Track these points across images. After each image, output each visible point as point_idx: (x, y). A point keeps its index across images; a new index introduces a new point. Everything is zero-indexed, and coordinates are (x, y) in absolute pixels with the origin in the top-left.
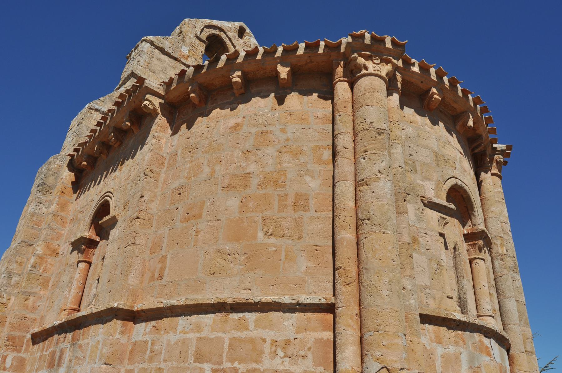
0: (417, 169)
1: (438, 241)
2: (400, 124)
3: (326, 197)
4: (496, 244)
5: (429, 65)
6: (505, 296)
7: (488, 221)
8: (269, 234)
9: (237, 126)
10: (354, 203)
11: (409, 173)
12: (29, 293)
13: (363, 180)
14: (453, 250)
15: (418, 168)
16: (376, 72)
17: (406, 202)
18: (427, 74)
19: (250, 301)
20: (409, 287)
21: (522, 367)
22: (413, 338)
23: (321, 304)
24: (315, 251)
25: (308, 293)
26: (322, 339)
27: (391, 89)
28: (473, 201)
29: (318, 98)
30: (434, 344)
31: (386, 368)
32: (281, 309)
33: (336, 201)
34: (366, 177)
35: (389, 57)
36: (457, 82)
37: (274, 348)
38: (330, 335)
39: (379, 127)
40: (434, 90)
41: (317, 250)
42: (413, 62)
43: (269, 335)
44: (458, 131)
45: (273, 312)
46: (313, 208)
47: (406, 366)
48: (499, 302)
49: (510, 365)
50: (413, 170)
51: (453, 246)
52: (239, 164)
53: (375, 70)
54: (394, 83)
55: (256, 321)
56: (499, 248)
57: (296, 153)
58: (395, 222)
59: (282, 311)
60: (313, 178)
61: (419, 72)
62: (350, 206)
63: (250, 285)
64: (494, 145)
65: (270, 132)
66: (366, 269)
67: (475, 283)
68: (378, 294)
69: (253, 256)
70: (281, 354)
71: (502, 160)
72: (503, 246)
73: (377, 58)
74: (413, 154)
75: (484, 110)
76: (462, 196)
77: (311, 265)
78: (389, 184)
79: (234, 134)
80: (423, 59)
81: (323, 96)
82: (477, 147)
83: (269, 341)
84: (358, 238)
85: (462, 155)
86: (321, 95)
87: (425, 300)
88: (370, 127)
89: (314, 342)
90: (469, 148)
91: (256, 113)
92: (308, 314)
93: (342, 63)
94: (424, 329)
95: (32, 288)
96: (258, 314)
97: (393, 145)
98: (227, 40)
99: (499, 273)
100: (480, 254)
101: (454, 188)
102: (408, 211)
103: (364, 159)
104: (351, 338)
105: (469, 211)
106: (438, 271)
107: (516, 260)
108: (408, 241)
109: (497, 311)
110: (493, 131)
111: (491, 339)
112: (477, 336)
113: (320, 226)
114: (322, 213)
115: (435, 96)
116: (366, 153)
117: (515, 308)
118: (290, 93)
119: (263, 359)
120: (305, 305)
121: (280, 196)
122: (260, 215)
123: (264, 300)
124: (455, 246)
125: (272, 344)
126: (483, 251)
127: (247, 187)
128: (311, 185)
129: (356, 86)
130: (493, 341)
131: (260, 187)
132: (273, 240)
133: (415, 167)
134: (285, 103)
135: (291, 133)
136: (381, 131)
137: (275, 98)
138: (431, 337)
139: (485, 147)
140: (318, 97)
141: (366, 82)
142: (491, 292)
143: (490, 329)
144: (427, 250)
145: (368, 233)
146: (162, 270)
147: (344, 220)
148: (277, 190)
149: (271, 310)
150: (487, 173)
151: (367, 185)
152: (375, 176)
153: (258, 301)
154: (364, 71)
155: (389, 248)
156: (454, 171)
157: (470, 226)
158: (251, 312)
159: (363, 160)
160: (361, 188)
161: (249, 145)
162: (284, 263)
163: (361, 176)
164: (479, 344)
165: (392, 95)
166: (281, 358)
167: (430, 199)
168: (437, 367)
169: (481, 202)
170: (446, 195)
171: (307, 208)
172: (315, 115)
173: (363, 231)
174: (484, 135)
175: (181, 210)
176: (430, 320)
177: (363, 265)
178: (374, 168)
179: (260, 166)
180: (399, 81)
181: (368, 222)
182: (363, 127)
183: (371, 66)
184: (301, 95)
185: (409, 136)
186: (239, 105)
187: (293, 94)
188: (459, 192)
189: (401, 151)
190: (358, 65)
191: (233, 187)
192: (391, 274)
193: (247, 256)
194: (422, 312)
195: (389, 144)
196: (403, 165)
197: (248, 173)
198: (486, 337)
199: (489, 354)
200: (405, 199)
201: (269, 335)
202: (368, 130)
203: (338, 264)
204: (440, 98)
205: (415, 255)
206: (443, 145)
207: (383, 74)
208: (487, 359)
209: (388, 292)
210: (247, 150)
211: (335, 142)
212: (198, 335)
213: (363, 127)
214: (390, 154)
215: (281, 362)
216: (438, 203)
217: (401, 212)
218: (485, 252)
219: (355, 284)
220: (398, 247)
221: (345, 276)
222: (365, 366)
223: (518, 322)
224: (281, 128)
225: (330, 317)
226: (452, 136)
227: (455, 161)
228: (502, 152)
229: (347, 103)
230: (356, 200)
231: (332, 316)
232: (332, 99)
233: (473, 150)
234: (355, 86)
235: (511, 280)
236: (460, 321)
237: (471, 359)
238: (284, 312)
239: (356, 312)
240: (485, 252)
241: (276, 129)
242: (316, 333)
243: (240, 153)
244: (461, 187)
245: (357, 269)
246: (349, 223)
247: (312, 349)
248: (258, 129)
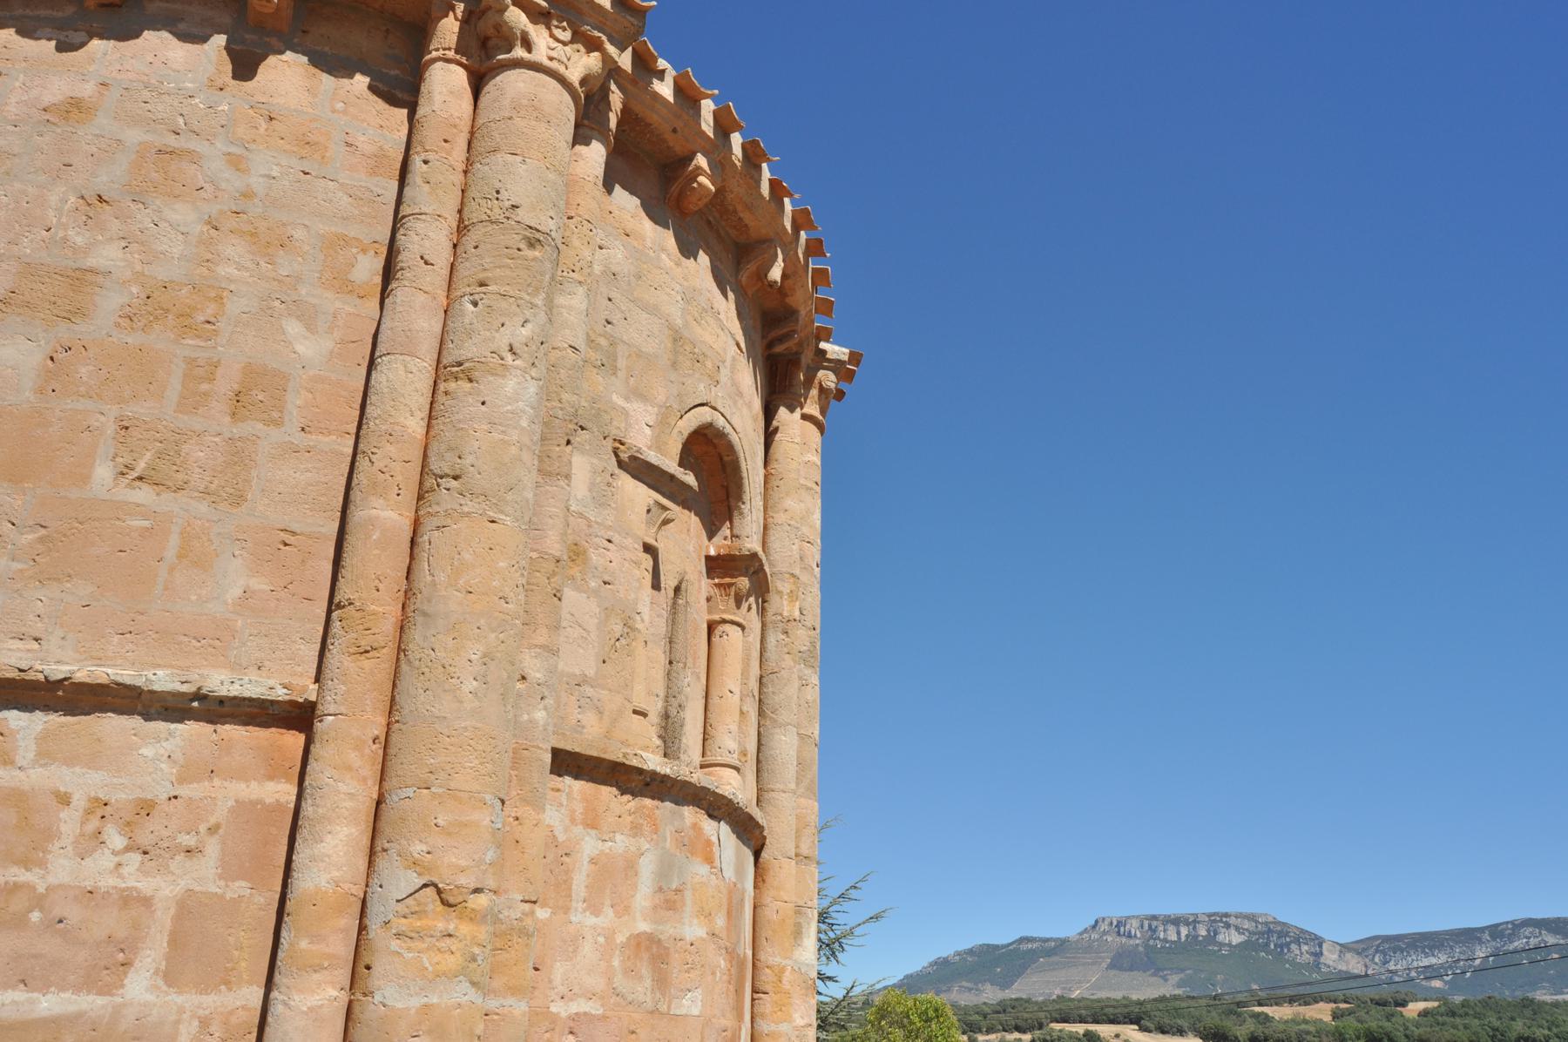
0: (619, 365)
1: (637, 563)
2: (594, 230)
3: (344, 393)
4: (780, 593)
5: (702, 89)
6: (775, 721)
7: (771, 532)
8: (136, 475)
9: (74, 109)
10: (424, 424)
11: (595, 370)
13: (460, 364)
14: (671, 594)
16: (554, 65)
17: (570, 447)
18: (691, 112)
19: (31, 676)
20: (538, 675)
21: (782, 893)
22: (526, 811)
23: (272, 702)
24: (281, 547)
25: (238, 667)
26: (260, 802)
27: (587, 125)
28: (745, 474)
29: (368, 91)
30: (578, 830)
31: (436, 886)
32: (140, 707)
33: (369, 409)
34: (470, 355)
35: (597, 34)
36: (763, 156)
37: (94, 823)
38: (285, 792)
39: (532, 225)
40: (701, 161)
41: (286, 545)
42: (661, 68)
43: (83, 783)
44: (742, 287)
45: (109, 714)
47: (491, 883)
48: (759, 734)
49: (756, 887)
50: (607, 366)
51: (673, 583)
52: (61, 234)
53: (551, 59)
54: (599, 111)
55: (44, 738)
56: (785, 603)
58: (530, 495)
59: (140, 714)
60: (310, 328)
61: (671, 99)
62: (410, 431)
63: (39, 625)
64: (823, 345)
65: (193, 157)
66: (425, 614)
67: (711, 683)
68: (447, 687)
69: (65, 535)
70: (117, 840)
71: (833, 386)
72: (795, 598)
73: (565, 24)
74: (614, 321)
75: (815, 248)
76: (721, 459)
77: (259, 584)
78: (532, 388)
79: (59, 130)
80: (689, 69)
81: (386, 89)
82: (781, 339)
83: (79, 801)
84: (417, 524)
85: (742, 351)
86: (380, 86)
87: (575, 714)
88: (508, 218)
89: (232, 811)
90: (763, 337)
91: (153, 81)
92: (227, 727)
93: (460, 7)
94: (558, 790)
96: (55, 719)
97: (566, 284)
99: (771, 665)
100: (736, 611)
101: (705, 435)
102: (573, 472)
103: (475, 304)
104: (348, 804)
105: (731, 499)
106: (623, 641)
107: (819, 637)
108: (558, 554)
109: (749, 756)
110: (826, 307)
111: (722, 822)
112: (690, 814)
113: (309, 474)
114: (320, 437)
115: (702, 179)
116: (483, 289)
117: (791, 752)
118: (282, 53)
119: (50, 857)
120: (221, 701)
121: (191, 362)
122: (113, 411)
123: (81, 676)
124: (680, 583)
125: (89, 812)
126: (745, 606)
127: (75, 314)
128: (300, 348)
129: (491, 89)
130: (725, 828)
131: (125, 322)
132: (143, 495)
133: (613, 357)
134: (256, 78)
135: (261, 176)
136: (538, 235)
137: (225, 52)
138: (574, 811)
139: (800, 344)
140: (371, 88)
141: (522, 85)
142: (745, 709)
143: (723, 797)
144: (605, 583)
145: (448, 514)
147: (384, 470)
148: (185, 342)
149: (103, 708)
150: (792, 410)
151: (471, 380)
152: (497, 360)
153: (61, 676)
154: (519, 52)
155: (501, 564)
156: (713, 389)
157: (725, 538)
158: (31, 711)
159: (471, 307)
160: (452, 385)
161: (107, 179)
162: (171, 570)
163: (456, 352)
164: (691, 832)
165: (587, 144)
166: (115, 853)
167: (638, 451)
168: (574, 887)
169: (765, 483)
170: (680, 446)
171: (275, 415)
172: (350, 140)
173: (436, 508)
174: (803, 312)
176: (579, 767)
177: (419, 602)
178: (497, 335)
179: (136, 256)
180: (613, 109)
181: (454, 484)
182: (488, 212)
183: (544, 43)
184: (316, 67)
185: (614, 269)
186: (91, 38)
187: (289, 56)
188: (715, 446)
189: (584, 306)
190: (504, 29)
191: (27, 305)
192: (493, 635)
193: (43, 532)
194: (561, 745)
195: (553, 278)
196: (580, 343)
197: (92, 271)
198: (711, 816)
199: (709, 860)
200: (571, 438)
201: (83, 783)
202: (501, 226)
203: (345, 592)
204: (713, 188)
205: (569, 593)
206: (696, 315)
207: (574, 76)
208: (703, 870)
209: (475, 683)
210: (99, 196)
211: (399, 236)
213: (488, 212)
214: (550, 306)
215: (112, 865)
216: (656, 464)
217: (551, 471)
218: (749, 609)
219: (388, 653)
220: (527, 566)
221: (361, 627)
222: (375, 881)
223: (793, 786)
224: (229, 154)
225: (296, 740)
226: (726, 297)
227: (720, 364)
228: (837, 367)
229: (455, 130)
230: (430, 417)
231: (301, 738)
232: (412, 109)
233: (770, 345)
234: (486, 89)
235: (796, 684)
236: (654, 774)
237: (665, 869)
238: (148, 717)
239: (376, 732)
240: (749, 609)
242: (243, 786)
243: (73, 199)
244: (721, 435)
245: (399, 613)
246: (399, 478)
247: (221, 831)
248: (149, 137)
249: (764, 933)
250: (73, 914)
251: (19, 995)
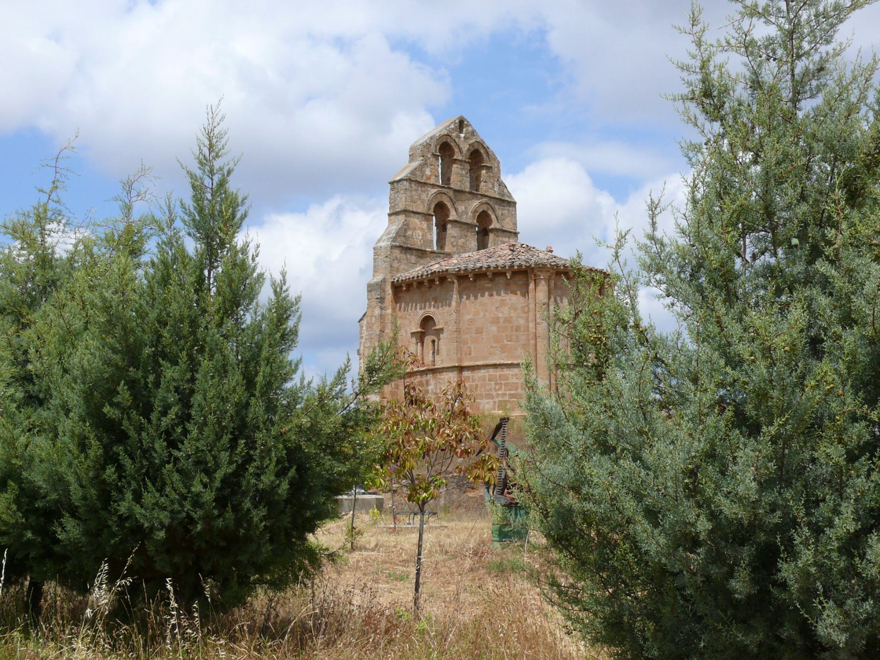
43: (511, 373)
57: (515, 309)
65: (505, 300)
98: (453, 144)
161: (497, 305)
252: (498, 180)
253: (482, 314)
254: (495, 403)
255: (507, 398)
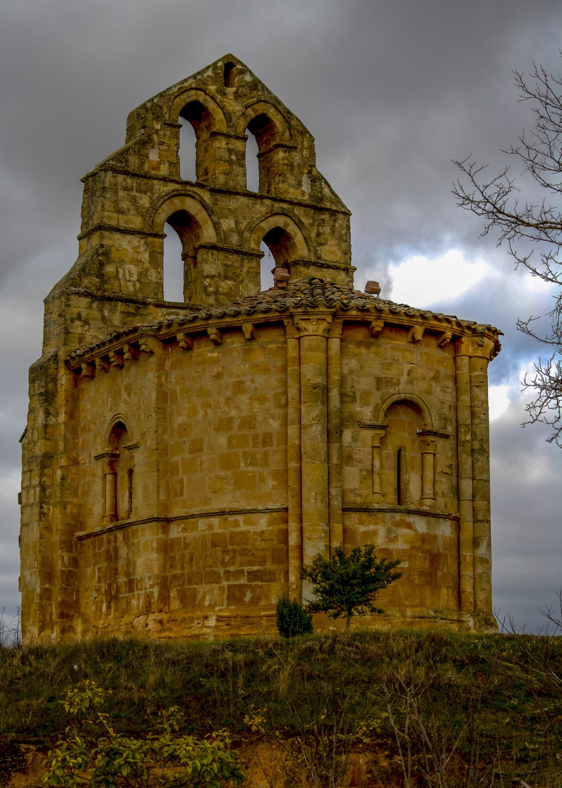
9: (219, 376)
12: (66, 502)
15: (358, 398)
25: (274, 503)
46: (275, 443)
57: (262, 400)
60: (275, 420)
77: (275, 483)
95: (66, 498)
121: (253, 435)
127: (230, 429)
132: (250, 468)
146: (182, 489)
161: (229, 393)
175: (188, 444)
197: (231, 417)
208: (408, 531)
212: (211, 532)
237: (389, 531)
241: (247, 379)
249: (461, 545)
250: (255, 552)
251: (250, 567)
252: (310, 172)
253: (202, 413)
254: (222, 589)
255: (243, 581)
